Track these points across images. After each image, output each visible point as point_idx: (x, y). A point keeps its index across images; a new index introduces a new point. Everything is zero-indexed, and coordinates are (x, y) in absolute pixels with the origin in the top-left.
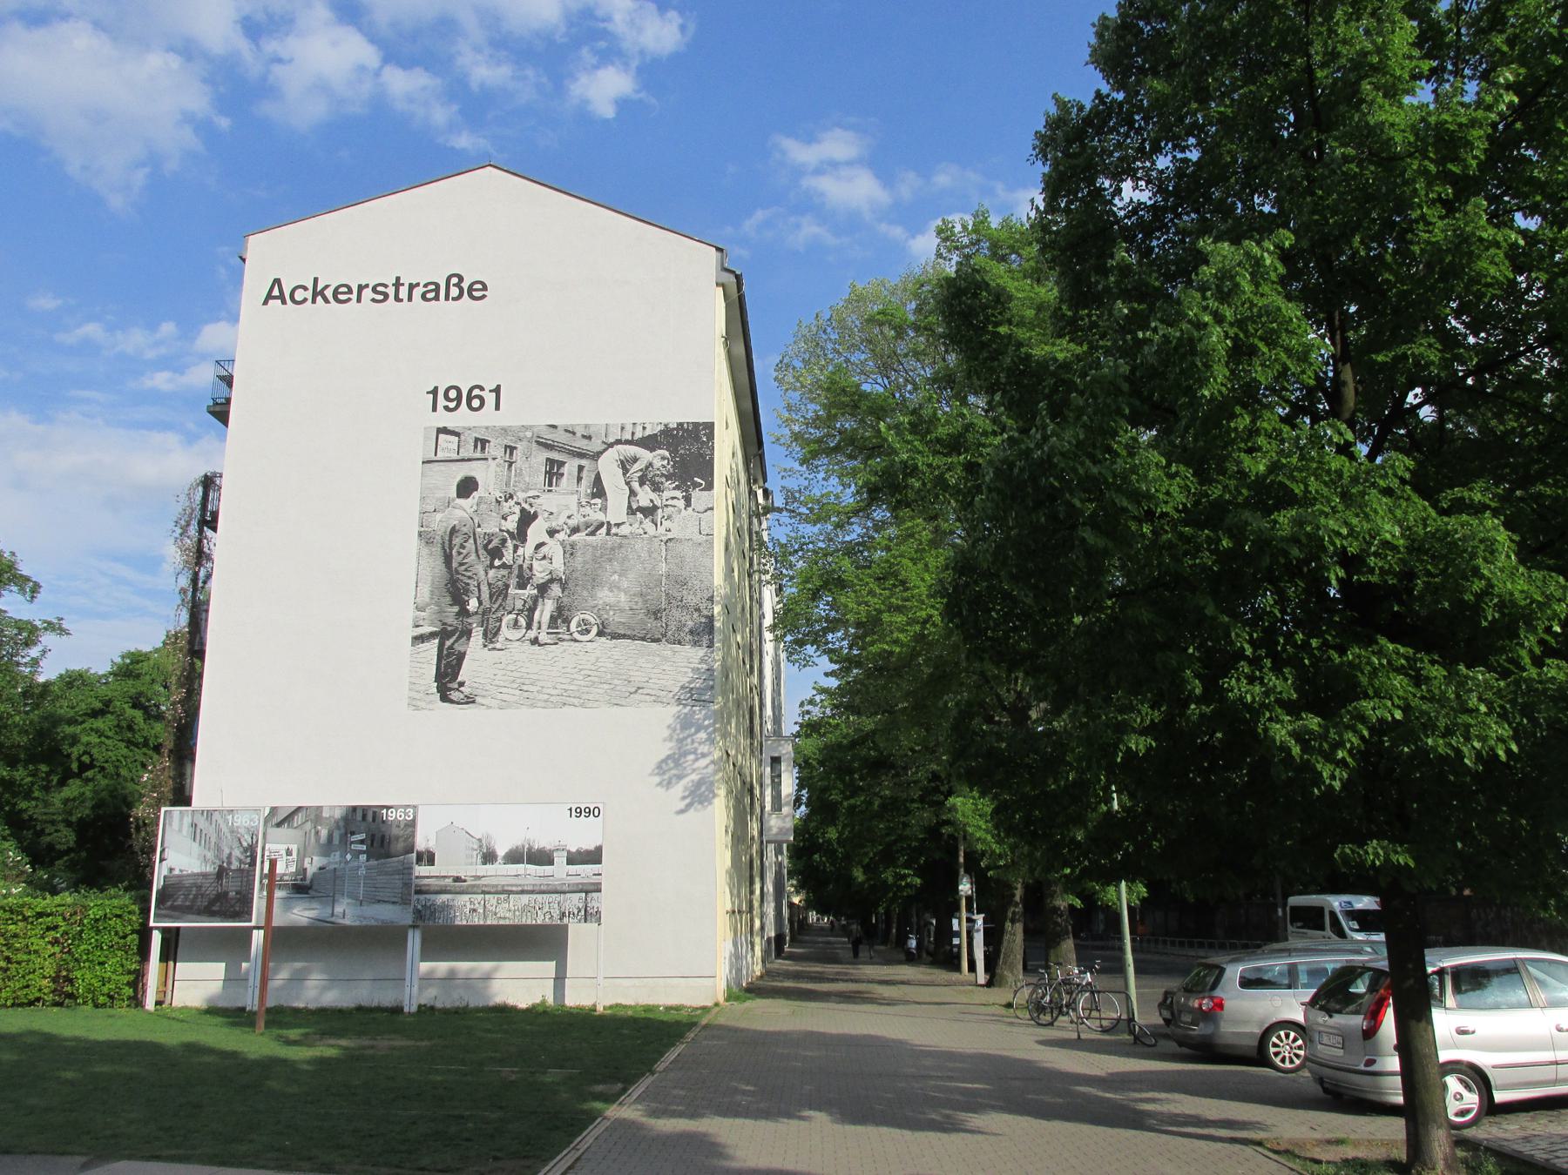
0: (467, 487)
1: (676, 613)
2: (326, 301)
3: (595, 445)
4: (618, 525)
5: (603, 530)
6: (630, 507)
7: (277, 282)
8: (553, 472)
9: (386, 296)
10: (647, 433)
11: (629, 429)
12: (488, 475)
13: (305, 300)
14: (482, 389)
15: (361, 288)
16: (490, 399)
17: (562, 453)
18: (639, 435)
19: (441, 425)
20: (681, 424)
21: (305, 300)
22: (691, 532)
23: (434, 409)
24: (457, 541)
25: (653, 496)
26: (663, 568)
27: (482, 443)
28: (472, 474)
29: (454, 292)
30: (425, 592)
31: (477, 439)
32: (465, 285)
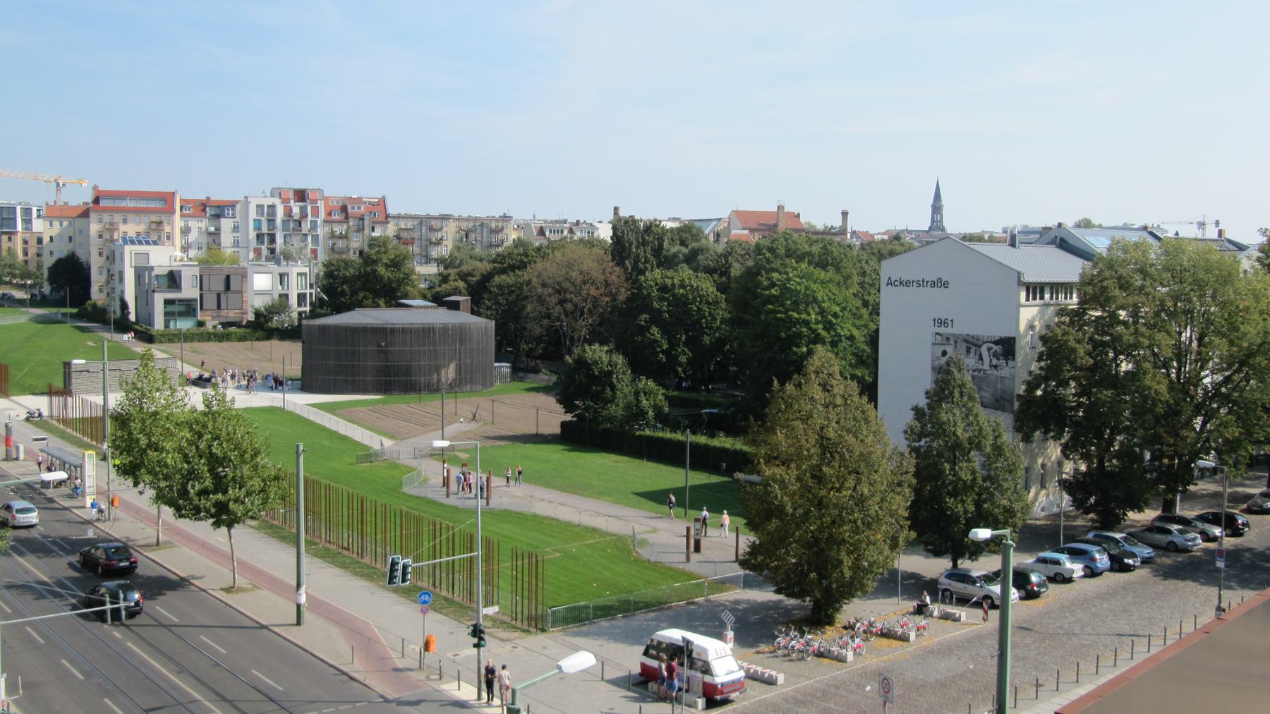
0: (944, 353)
8: (968, 350)
12: (949, 349)
17: (972, 344)
27: (948, 339)
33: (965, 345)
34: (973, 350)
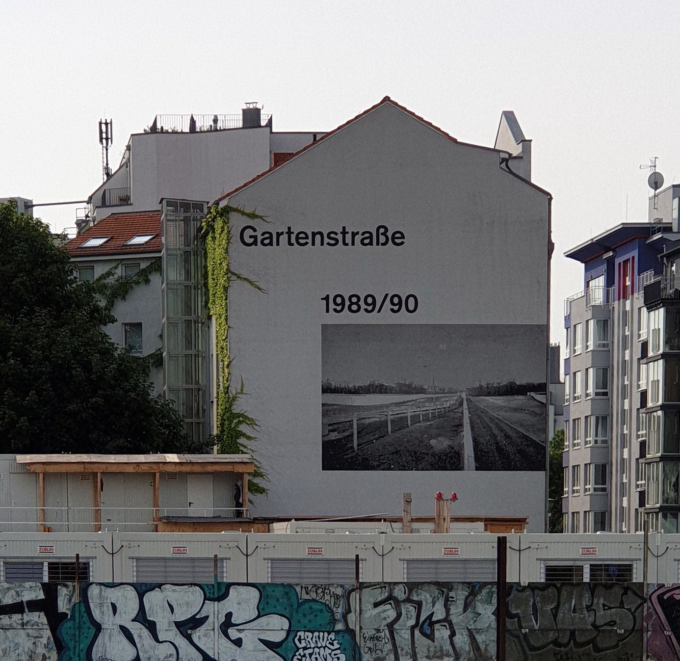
23: (328, 311)
29: (382, 239)
32: (390, 234)
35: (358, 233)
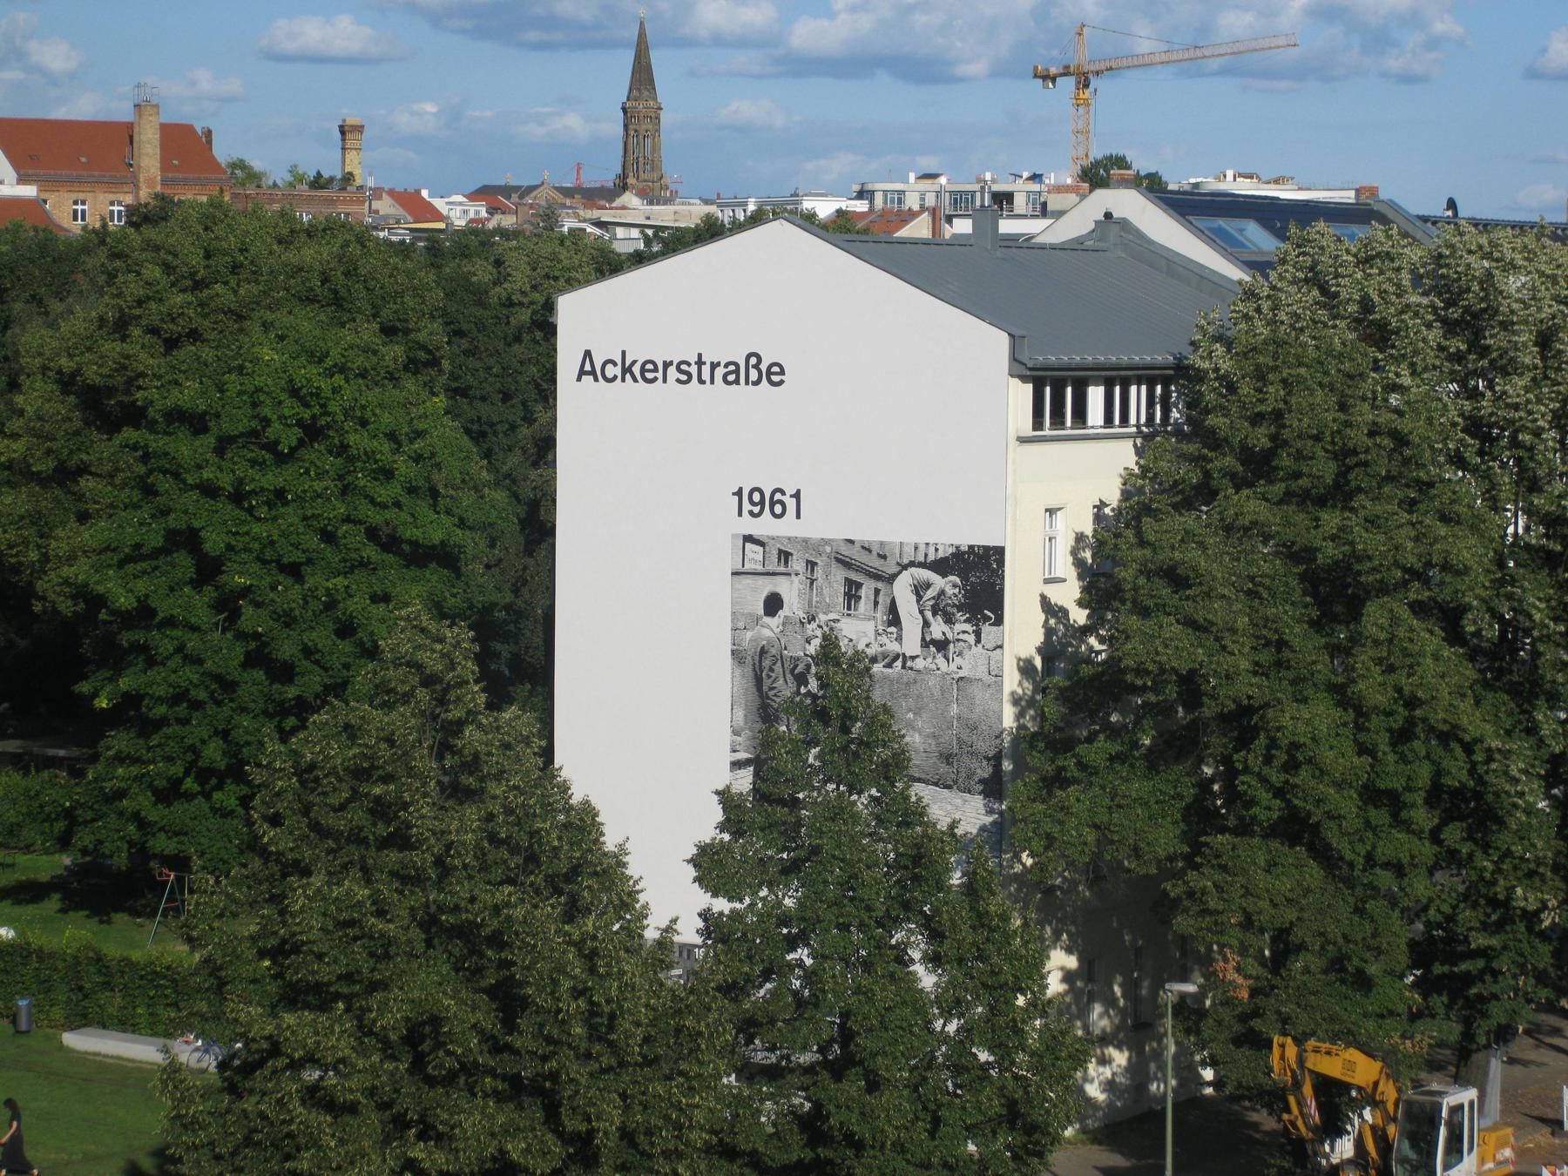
0: (773, 604)
1: (966, 759)
2: (635, 380)
3: (891, 568)
4: (913, 658)
5: (899, 663)
6: (923, 639)
7: (588, 354)
8: (852, 594)
9: (689, 375)
10: (941, 554)
11: (922, 548)
12: (791, 591)
13: (615, 377)
14: (783, 493)
15: (667, 365)
16: (791, 504)
17: (862, 570)
18: (931, 557)
19: (747, 533)
20: (971, 547)
21: (615, 377)
22: (981, 672)
23: (740, 514)
24: (767, 663)
25: (946, 628)
26: (954, 709)
27: (785, 556)
28: (778, 590)
29: (754, 375)
30: (740, 714)
31: (780, 551)
32: (764, 367)
33: (839, 574)
34: (866, 591)
35: (718, 364)
